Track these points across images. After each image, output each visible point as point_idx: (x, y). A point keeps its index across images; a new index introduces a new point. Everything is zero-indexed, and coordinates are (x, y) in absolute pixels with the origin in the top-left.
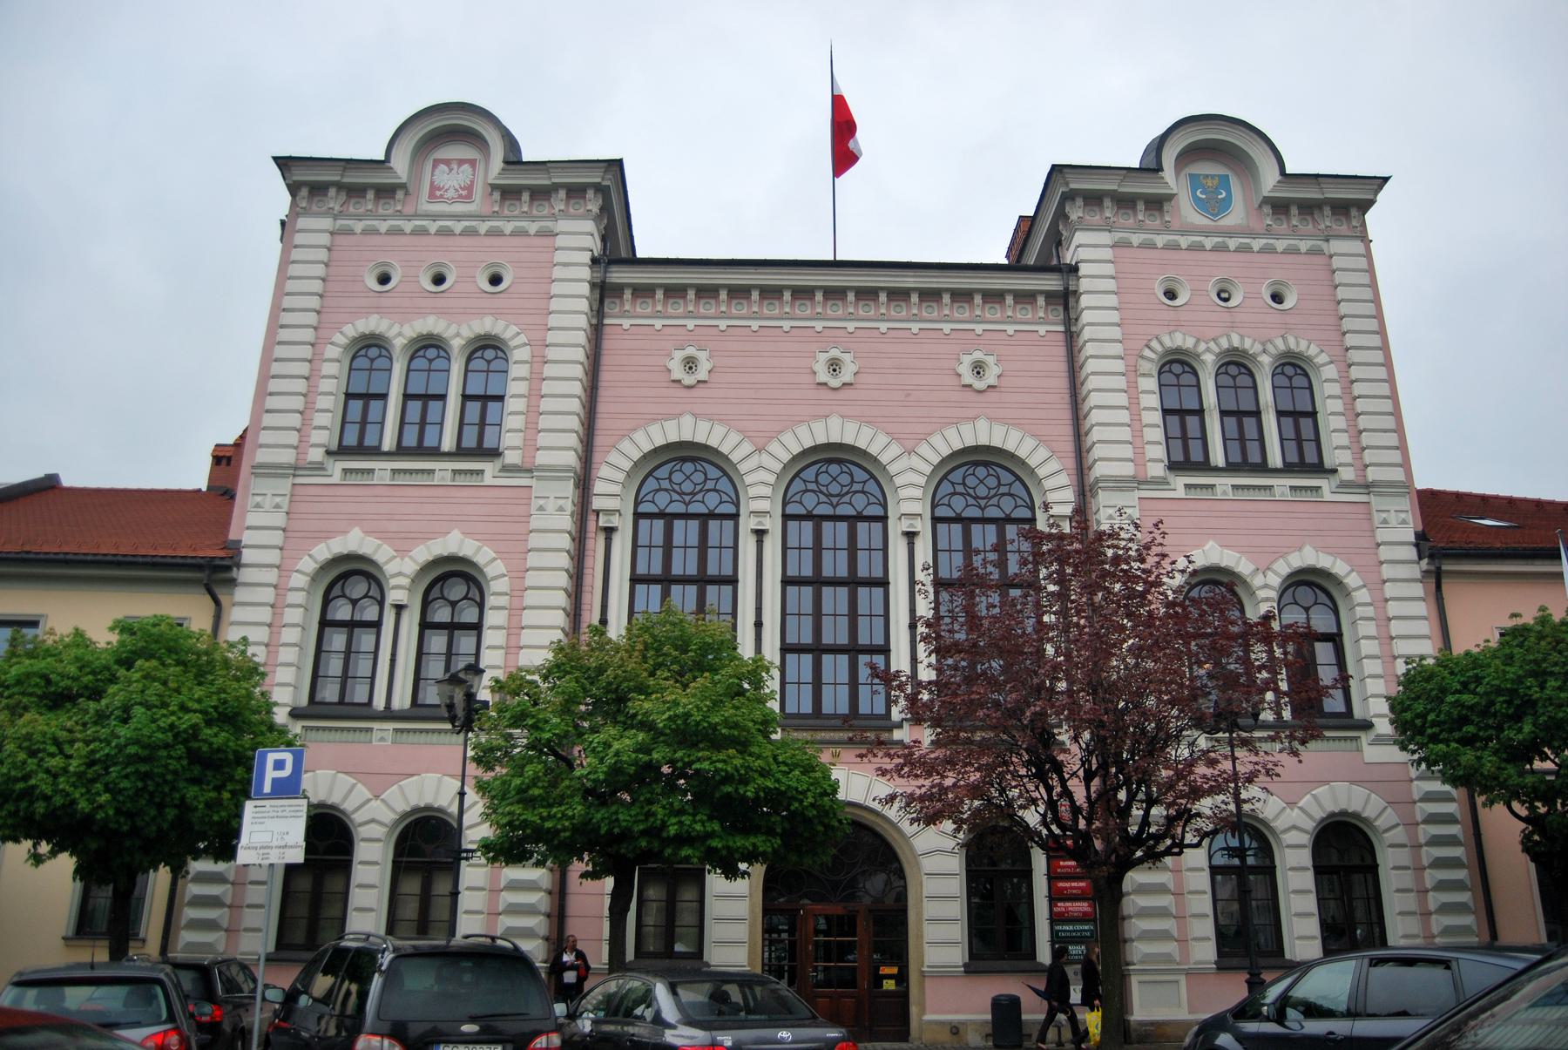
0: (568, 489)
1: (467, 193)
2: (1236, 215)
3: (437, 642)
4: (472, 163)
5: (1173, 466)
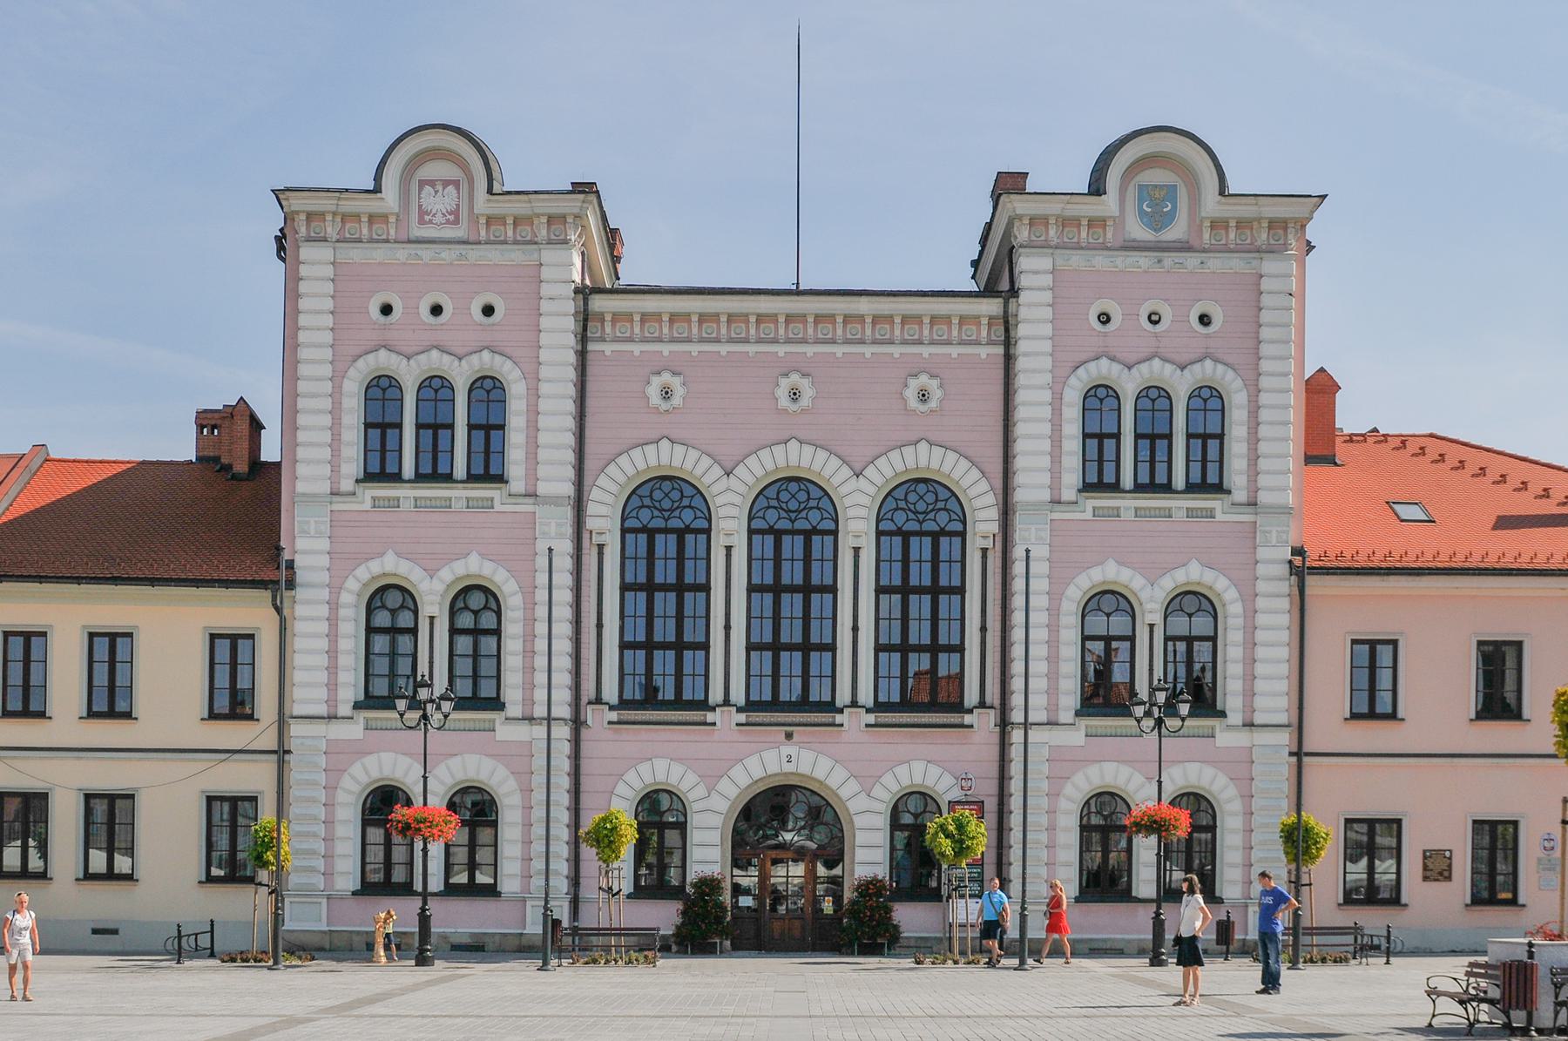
0: (568, 513)
1: (455, 217)
3: (464, 643)
4: (456, 184)
5: (1087, 487)
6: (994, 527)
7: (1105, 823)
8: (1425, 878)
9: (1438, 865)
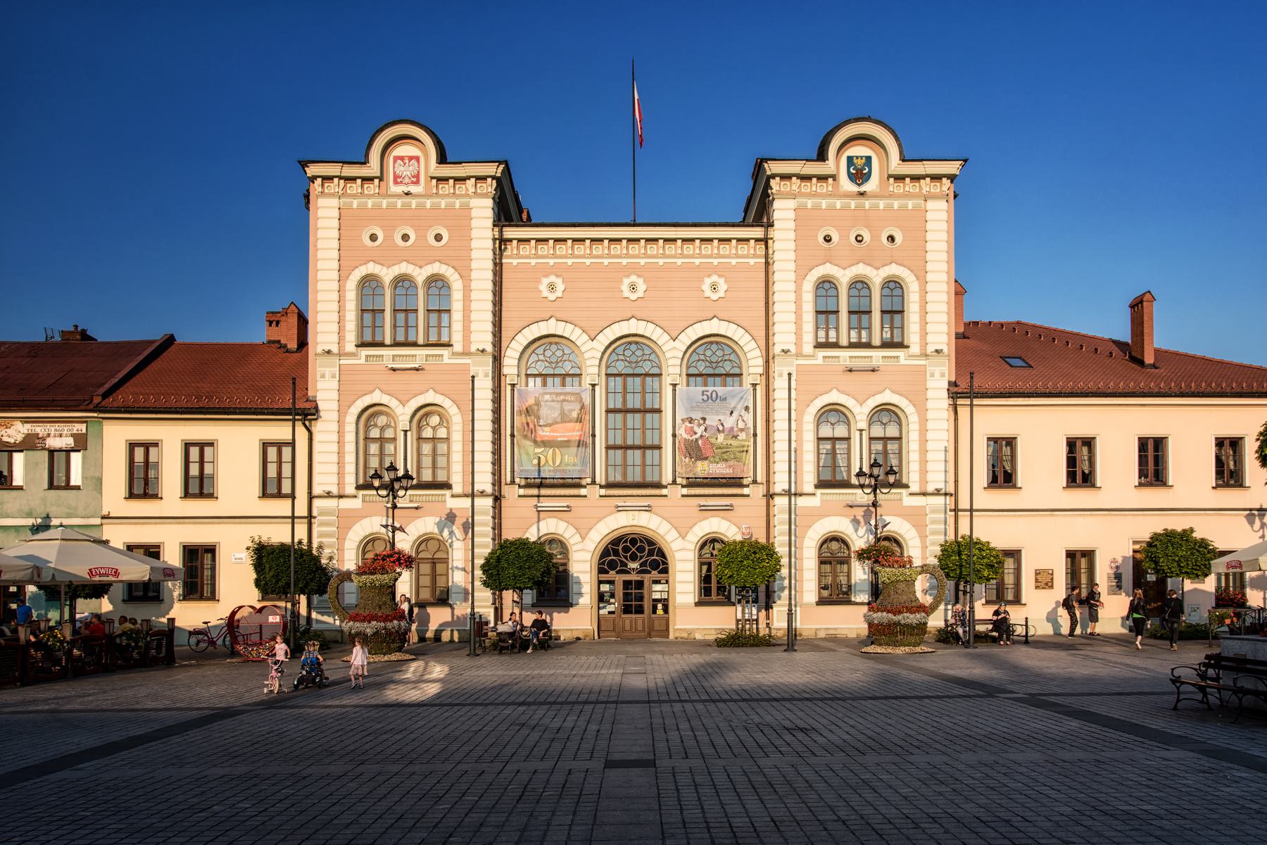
2: (871, 186)
4: (417, 159)
6: (761, 370)
7: (833, 553)
8: (1037, 587)
9: (1042, 578)
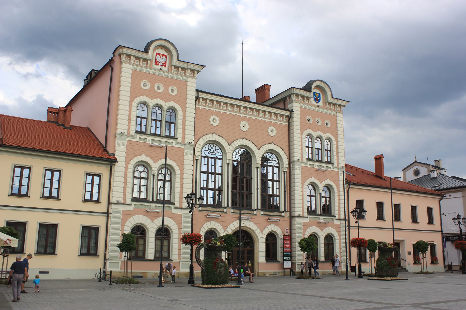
2: (320, 104)
4: (166, 56)
6: (288, 166)
